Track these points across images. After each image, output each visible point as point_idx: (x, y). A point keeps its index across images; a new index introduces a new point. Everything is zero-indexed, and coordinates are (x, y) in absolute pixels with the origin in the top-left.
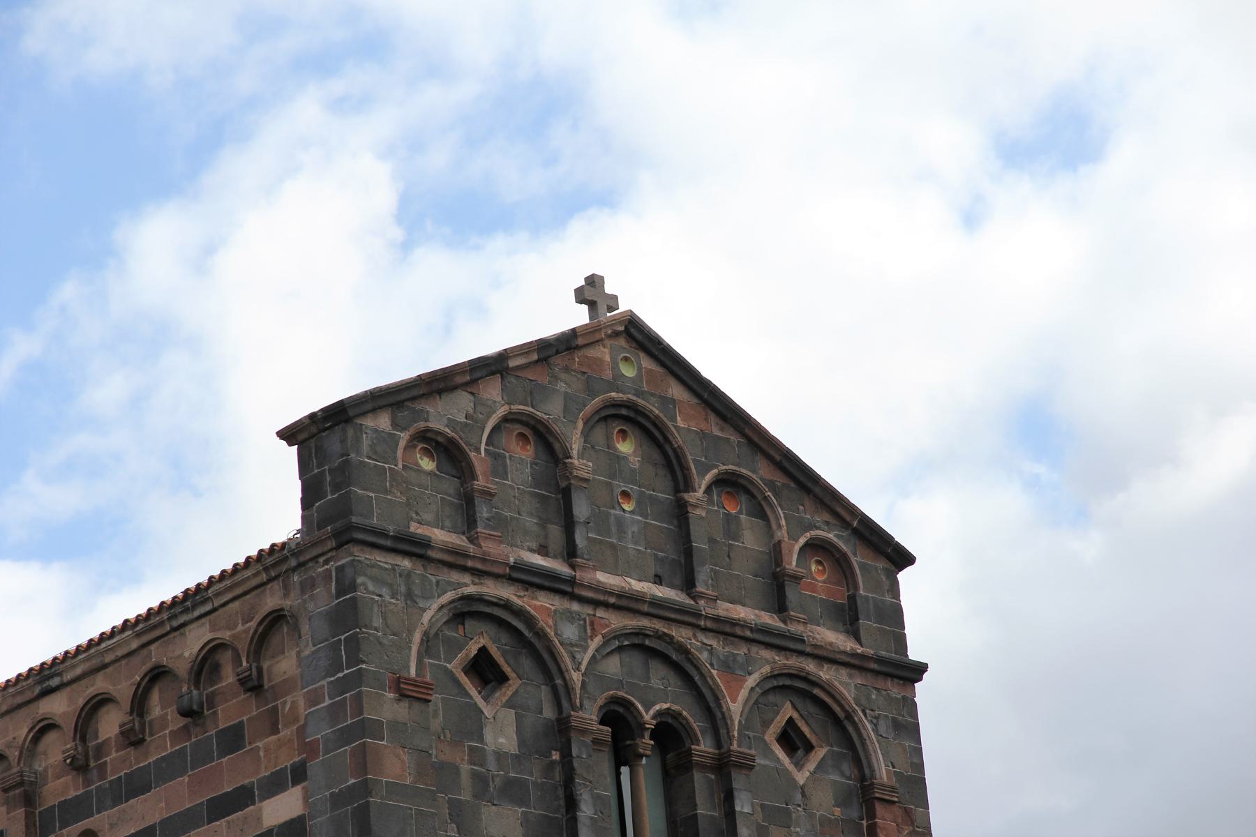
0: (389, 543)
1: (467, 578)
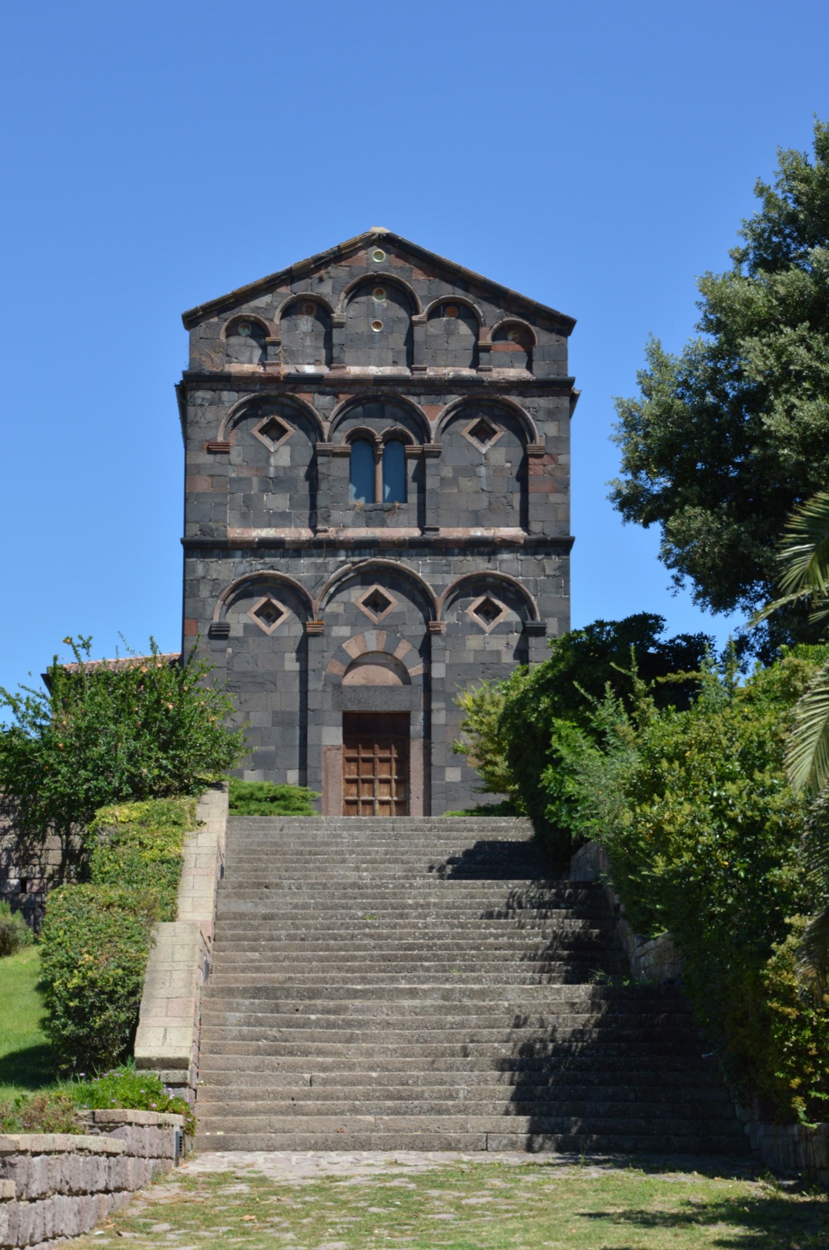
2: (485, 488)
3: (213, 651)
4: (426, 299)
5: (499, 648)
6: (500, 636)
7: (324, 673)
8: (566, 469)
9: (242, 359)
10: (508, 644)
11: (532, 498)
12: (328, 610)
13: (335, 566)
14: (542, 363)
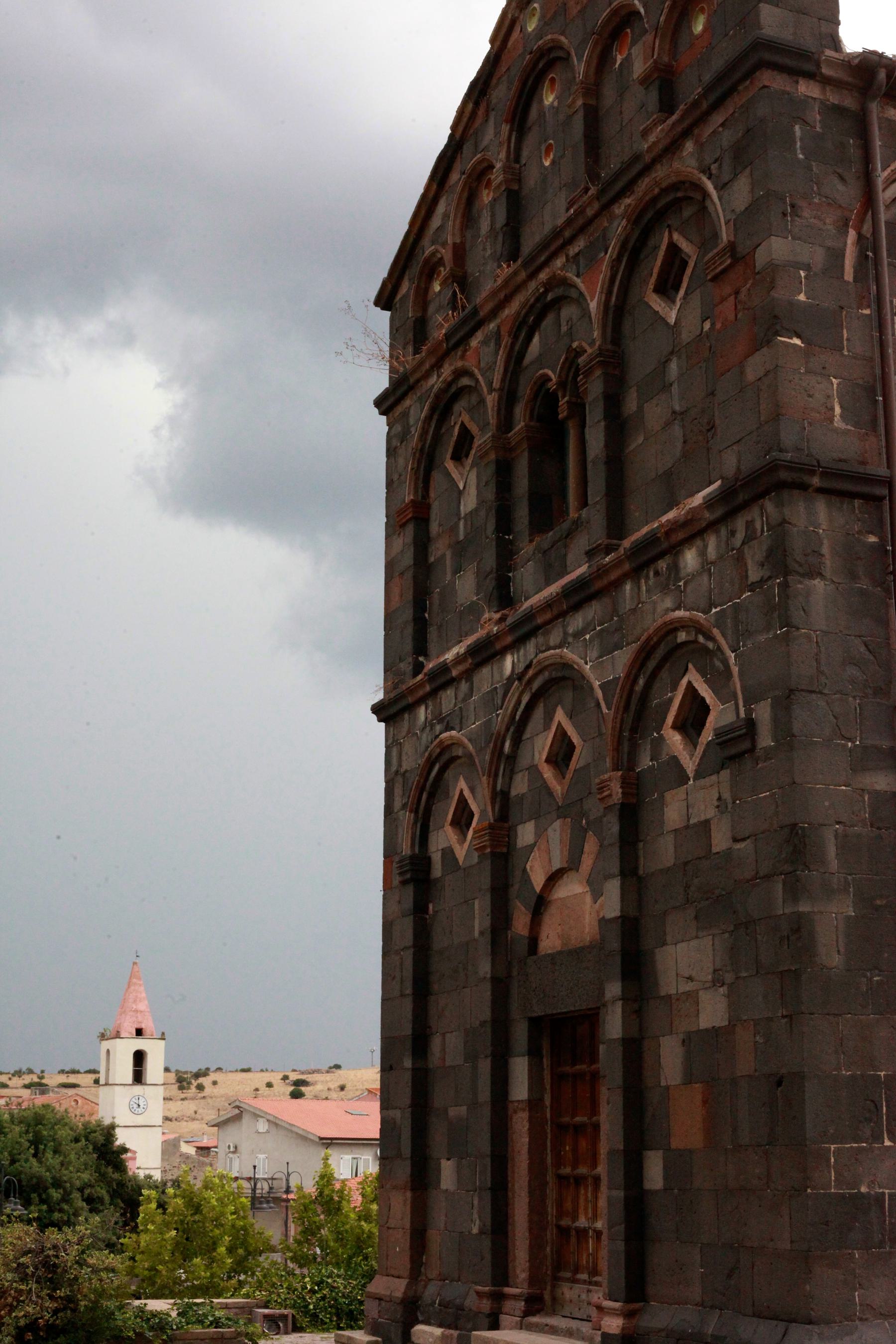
0: (391, 400)
2: (677, 408)
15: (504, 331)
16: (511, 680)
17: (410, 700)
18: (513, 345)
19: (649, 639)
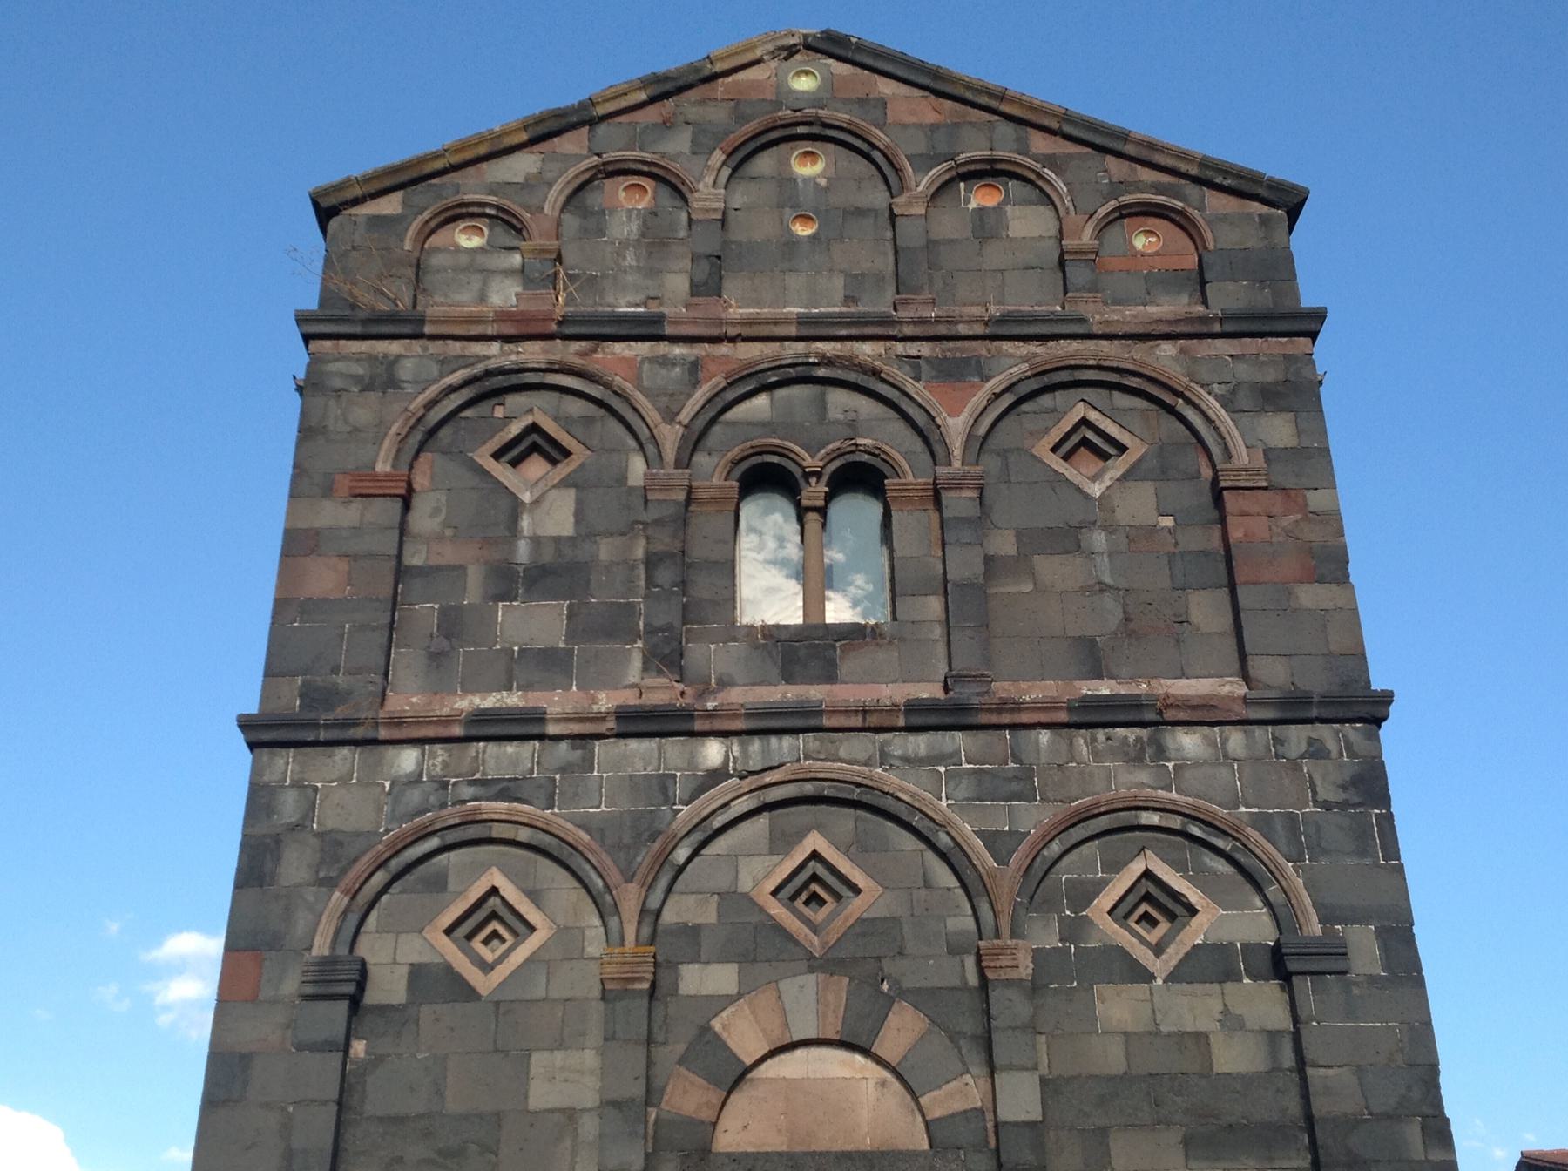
0: (358, 329)
1: (495, 348)
2: (1108, 580)
3: (300, 1047)
4: (924, 161)
5: (1205, 1025)
6: (1198, 987)
7: (653, 1114)
8: (1332, 520)
9: (458, 297)
10: (1225, 1011)
11: (1245, 596)
12: (668, 917)
13: (693, 785)
14: (1231, 286)
15: (712, 367)
16: (717, 776)
17: (383, 734)
18: (724, 389)
19: (1097, 805)
